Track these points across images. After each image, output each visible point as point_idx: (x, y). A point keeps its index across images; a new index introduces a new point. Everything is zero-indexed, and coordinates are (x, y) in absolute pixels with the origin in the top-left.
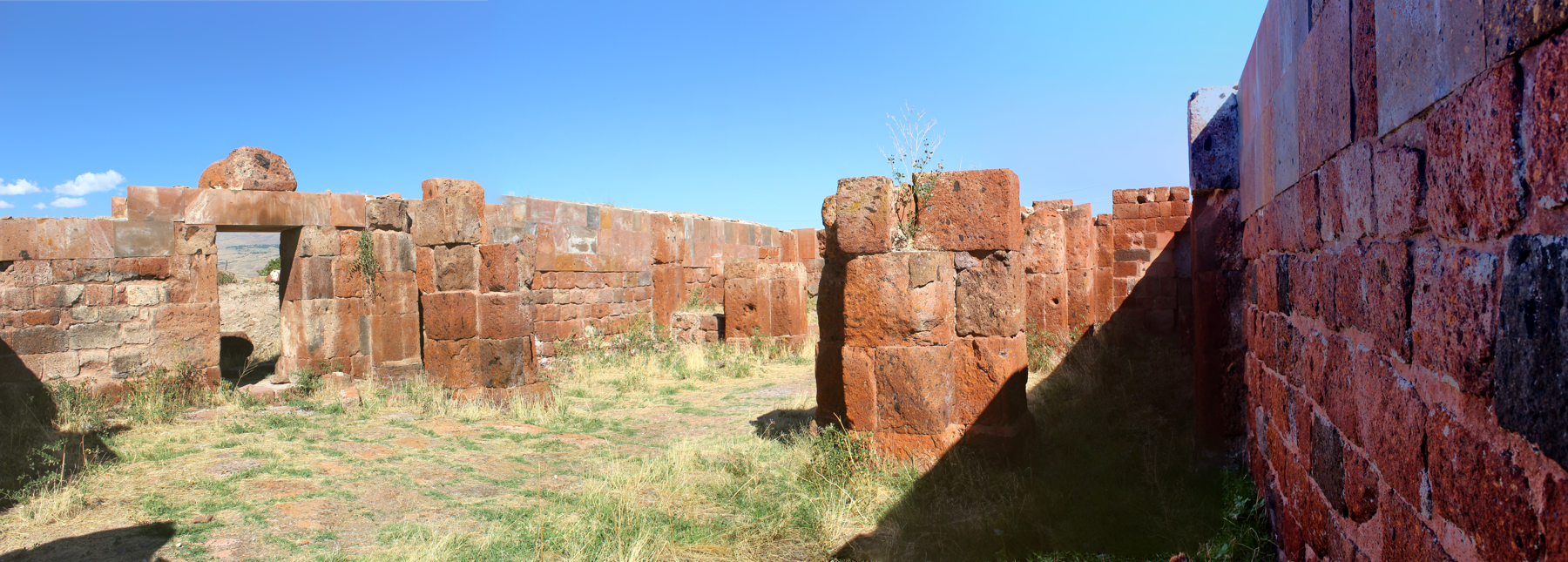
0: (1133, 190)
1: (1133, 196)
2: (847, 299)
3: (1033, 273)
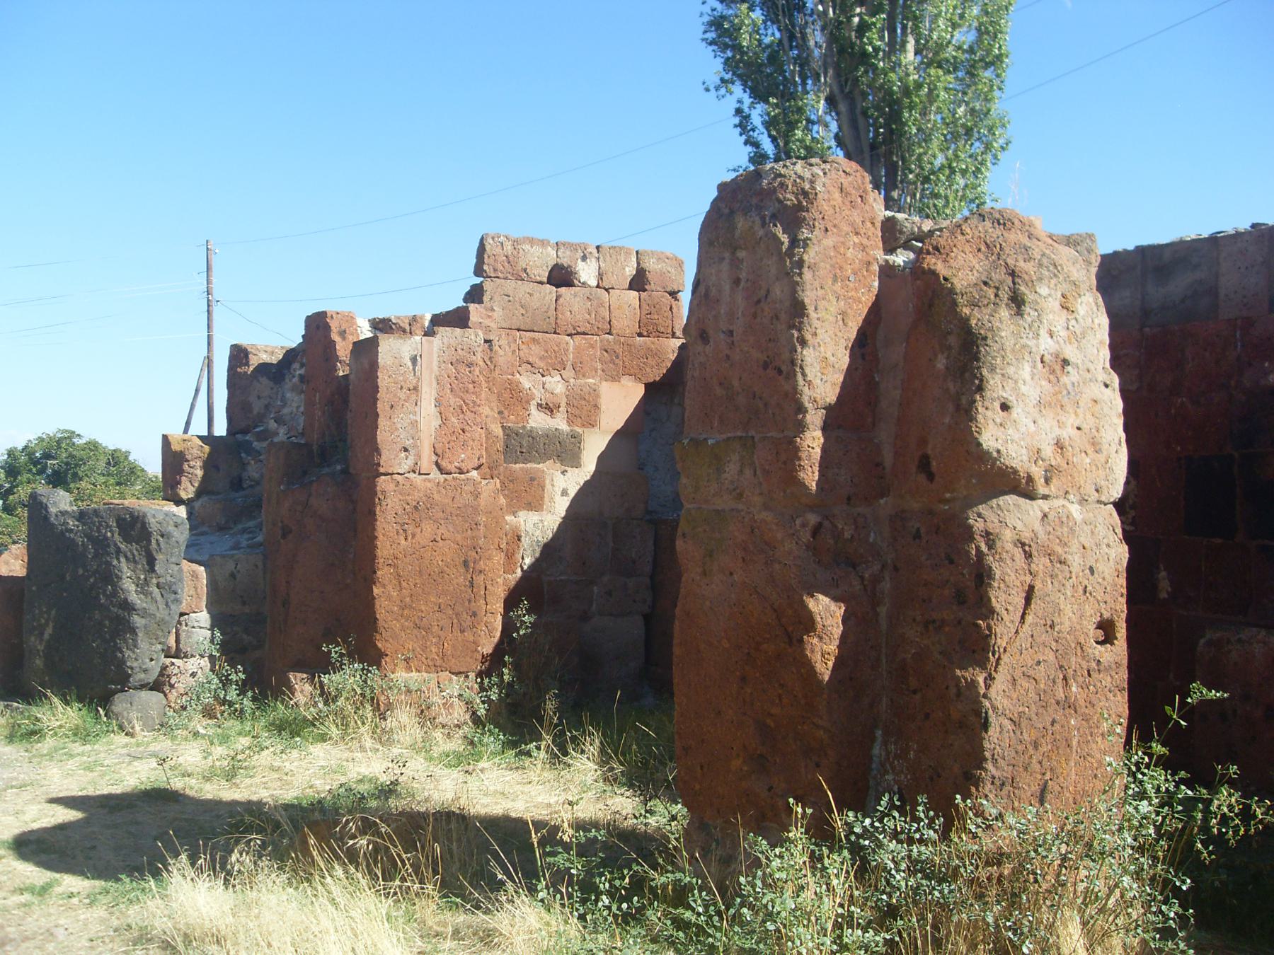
0: (544, 243)
1: (540, 261)
3: (1030, 495)
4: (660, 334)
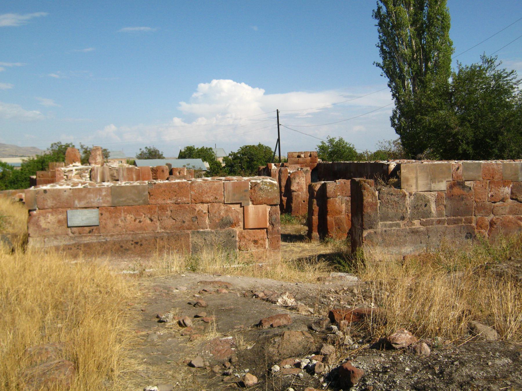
0: (296, 152)
1: (296, 155)
2: (328, 207)
4: (314, 163)
